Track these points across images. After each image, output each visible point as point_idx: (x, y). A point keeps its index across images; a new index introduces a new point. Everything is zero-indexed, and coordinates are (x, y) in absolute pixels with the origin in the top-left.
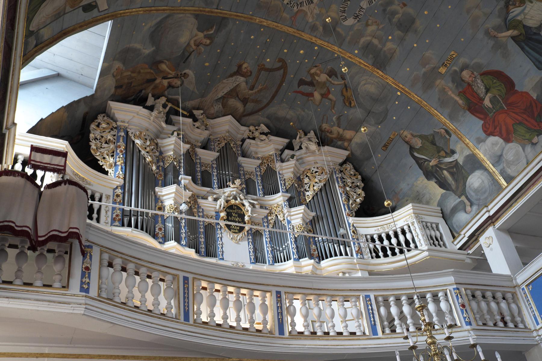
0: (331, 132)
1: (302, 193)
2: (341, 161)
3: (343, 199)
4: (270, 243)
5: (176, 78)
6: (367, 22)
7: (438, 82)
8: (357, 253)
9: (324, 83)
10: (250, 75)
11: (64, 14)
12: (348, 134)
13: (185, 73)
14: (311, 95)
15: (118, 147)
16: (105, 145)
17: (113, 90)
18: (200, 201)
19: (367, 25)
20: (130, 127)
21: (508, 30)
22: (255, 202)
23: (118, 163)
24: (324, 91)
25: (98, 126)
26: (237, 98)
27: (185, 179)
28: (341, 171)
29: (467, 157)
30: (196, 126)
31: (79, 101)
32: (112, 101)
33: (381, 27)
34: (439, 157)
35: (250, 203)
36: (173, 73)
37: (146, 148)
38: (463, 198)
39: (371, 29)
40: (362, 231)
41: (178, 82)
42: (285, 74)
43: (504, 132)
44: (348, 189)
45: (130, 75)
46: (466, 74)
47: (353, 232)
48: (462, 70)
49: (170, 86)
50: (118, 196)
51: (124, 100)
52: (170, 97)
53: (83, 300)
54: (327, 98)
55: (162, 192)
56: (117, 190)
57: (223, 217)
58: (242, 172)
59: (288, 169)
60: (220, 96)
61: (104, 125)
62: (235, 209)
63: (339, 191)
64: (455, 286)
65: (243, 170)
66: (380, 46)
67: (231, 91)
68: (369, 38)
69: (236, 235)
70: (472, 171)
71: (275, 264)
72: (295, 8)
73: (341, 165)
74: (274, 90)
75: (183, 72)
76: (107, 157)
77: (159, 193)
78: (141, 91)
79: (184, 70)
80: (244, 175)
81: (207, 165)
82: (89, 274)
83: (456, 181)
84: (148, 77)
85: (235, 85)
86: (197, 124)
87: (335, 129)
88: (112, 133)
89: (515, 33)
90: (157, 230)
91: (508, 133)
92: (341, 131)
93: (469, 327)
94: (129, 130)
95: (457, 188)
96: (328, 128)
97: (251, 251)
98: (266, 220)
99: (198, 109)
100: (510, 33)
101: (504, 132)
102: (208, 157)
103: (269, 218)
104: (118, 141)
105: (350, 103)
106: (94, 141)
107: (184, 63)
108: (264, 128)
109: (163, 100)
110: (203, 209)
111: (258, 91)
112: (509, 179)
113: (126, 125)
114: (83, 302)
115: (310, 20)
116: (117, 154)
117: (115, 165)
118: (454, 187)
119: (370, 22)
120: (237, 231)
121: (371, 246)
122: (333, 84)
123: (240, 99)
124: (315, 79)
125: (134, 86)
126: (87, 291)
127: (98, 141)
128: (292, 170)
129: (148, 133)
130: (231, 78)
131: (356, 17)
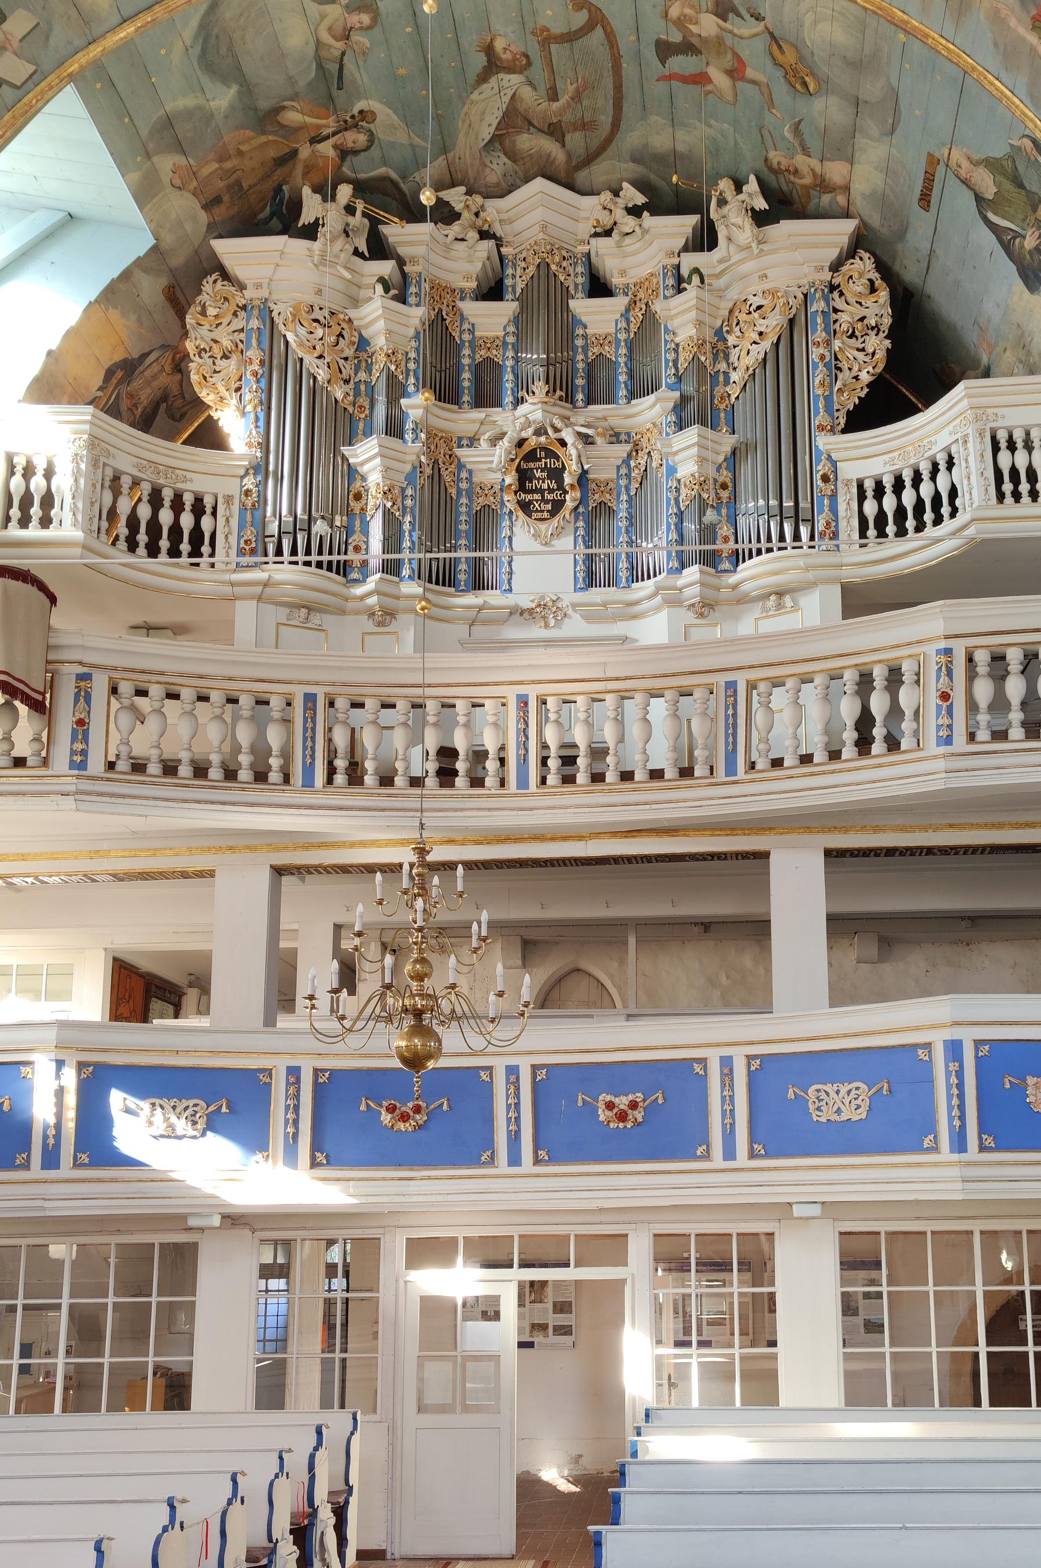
3: (817, 381)
4: (627, 532)
5: (346, 129)
9: (719, 41)
10: (529, 64)
13: (361, 112)
14: (701, 79)
16: (221, 364)
17: (203, 217)
20: (274, 297)
22: (590, 432)
24: (728, 61)
25: (203, 313)
26: (532, 129)
30: (451, 237)
31: (126, 275)
32: (220, 236)
35: (579, 434)
36: (330, 124)
37: (314, 348)
41: (355, 138)
42: (611, 38)
45: (221, 168)
47: (825, 479)
49: (344, 153)
51: (249, 226)
52: (362, 176)
54: (743, 79)
55: (356, 456)
57: (511, 485)
59: (682, 312)
61: (211, 311)
62: (540, 460)
67: (506, 115)
69: (543, 526)
71: (635, 585)
74: (608, 82)
75: (355, 111)
76: (227, 395)
77: (351, 461)
78: (278, 190)
79: (353, 105)
81: (490, 343)
84: (273, 153)
85: (506, 99)
92: (815, 163)
94: (272, 306)
98: (624, 471)
103: (632, 464)
105: (805, 84)
106: (197, 359)
107: (340, 88)
109: (345, 192)
110: (470, 472)
111: (572, 99)
113: (264, 293)
120: (546, 515)
122: (741, 38)
123: (540, 130)
124: (692, 34)
125: (250, 187)
127: (205, 356)
128: (693, 314)
129: (316, 301)
130: (485, 86)
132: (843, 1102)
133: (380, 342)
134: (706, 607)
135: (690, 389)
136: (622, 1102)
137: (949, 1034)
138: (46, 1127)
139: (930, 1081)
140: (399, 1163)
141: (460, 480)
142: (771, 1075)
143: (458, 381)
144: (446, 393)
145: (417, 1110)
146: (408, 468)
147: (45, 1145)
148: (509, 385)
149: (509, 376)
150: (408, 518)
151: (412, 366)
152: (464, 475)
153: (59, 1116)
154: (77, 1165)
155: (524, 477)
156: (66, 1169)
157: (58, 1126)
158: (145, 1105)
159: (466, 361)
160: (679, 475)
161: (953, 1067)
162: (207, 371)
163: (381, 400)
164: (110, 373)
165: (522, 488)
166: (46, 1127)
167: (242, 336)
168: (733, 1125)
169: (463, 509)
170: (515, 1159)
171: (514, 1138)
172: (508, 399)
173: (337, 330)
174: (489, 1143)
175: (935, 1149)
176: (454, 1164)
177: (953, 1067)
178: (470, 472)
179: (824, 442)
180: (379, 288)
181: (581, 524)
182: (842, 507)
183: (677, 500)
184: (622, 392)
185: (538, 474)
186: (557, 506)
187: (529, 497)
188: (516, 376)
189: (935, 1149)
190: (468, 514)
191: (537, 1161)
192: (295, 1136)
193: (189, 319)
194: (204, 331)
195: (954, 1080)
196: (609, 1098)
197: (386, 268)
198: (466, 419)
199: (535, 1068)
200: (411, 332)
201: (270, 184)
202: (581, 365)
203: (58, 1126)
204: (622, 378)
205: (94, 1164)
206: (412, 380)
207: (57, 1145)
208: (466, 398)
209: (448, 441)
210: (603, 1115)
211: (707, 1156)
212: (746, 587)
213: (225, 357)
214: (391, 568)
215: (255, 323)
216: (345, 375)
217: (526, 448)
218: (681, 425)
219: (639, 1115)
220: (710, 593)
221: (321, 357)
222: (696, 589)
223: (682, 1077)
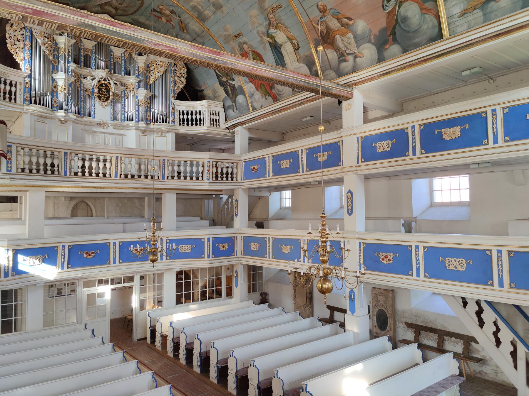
7: (232, 42)
8: (172, 121)
15: (25, 45)
16: (17, 43)
18: (83, 80)
21: (268, 37)
23: (26, 58)
25: (11, 26)
27: (72, 66)
28: (175, 64)
29: (239, 86)
34: (227, 78)
38: (234, 104)
40: (178, 108)
43: (256, 84)
44: (176, 78)
46: (245, 46)
47: (173, 108)
48: (244, 43)
50: (27, 83)
56: (26, 79)
58: (112, 57)
60: (98, 4)
63: (171, 79)
64: (208, 160)
66: (202, 10)
68: (196, 4)
69: (104, 103)
70: (240, 94)
82: (11, 162)
83: (233, 94)
88: (22, 32)
89: (271, 41)
91: (258, 86)
93: (208, 181)
95: (232, 97)
100: (268, 39)
101: (256, 84)
104: (26, 40)
106: (9, 39)
112: (254, 109)
114: (9, 177)
116: (26, 51)
117: (24, 59)
118: (231, 96)
121: (181, 117)
126: (10, 171)
127: (12, 39)
132: (187, 249)
134: (144, 132)
137: (208, 237)
138: (5, 267)
139: (204, 245)
140: (88, 266)
141: (81, 86)
144: (77, 62)
146: (70, 82)
153: (8, 263)
154: (12, 275)
157: (8, 266)
158: (28, 258)
163: (62, 61)
166: (5, 267)
170: (114, 262)
171: (115, 258)
174: (109, 259)
175: (204, 258)
176: (100, 265)
182: (176, 116)
186: (107, 99)
189: (204, 258)
191: (119, 263)
198: (85, 71)
199: (119, 242)
205: (16, 274)
207: (8, 271)
219: (142, 252)
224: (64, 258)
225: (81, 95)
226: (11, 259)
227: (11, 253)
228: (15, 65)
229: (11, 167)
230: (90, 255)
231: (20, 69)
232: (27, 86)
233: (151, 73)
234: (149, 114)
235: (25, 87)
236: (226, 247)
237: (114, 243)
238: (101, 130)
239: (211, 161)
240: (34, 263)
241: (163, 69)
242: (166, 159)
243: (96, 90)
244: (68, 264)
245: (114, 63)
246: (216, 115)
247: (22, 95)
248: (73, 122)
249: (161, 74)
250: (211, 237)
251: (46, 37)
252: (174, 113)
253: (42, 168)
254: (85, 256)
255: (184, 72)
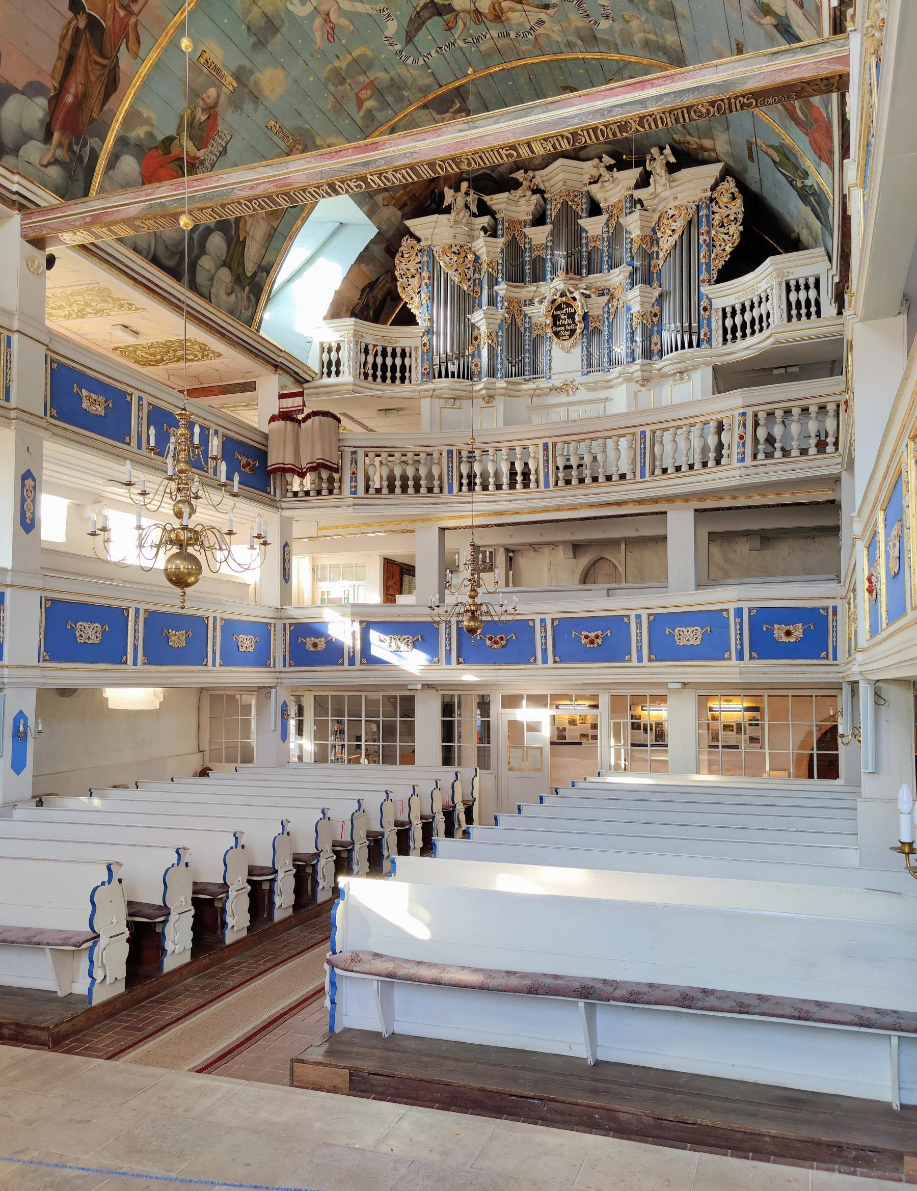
0: (688, 143)
1: (655, 255)
2: (712, 181)
6: (624, 19)
11: (275, 229)
12: (707, 143)
17: (399, 213)
19: (628, 22)
20: (434, 243)
22: (587, 292)
23: (424, 302)
25: (402, 256)
27: (502, 289)
33: (643, 19)
39: (635, 24)
40: (718, 304)
50: (425, 345)
53: (351, 501)
61: (406, 256)
64: (741, 411)
65: (587, 238)
68: (641, 35)
69: (566, 343)
72: (529, 36)
73: (713, 189)
78: (433, 192)
80: (587, 244)
82: (356, 478)
86: (520, 192)
87: (689, 138)
90: (474, 368)
93: (739, 464)
96: (682, 140)
97: (585, 358)
99: (518, 169)
102: (539, 235)
108: (608, 160)
109: (464, 186)
110: (530, 318)
113: (429, 243)
114: (351, 503)
115: (559, 39)
119: (627, 18)
121: (729, 323)
126: (355, 493)
131: (607, 17)
132: (690, 636)
133: (484, 258)
134: (645, 381)
135: (637, 263)
136: (592, 635)
137: (736, 605)
138: (349, 648)
139: (729, 626)
140: (495, 663)
142: (662, 624)
143: (524, 270)
145: (502, 639)
146: (499, 321)
147: (349, 656)
148: (549, 269)
149: (549, 264)
150: (500, 348)
151: (500, 267)
152: (527, 320)
153: (354, 644)
154: (362, 663)
155: (556, 318)
156: (358, 665)
158: (388, 638)
159: (527, 259)
160: (632, 312)
161: (738, 620)
162: (405, 285)
163: (485, 287)
164: (363, 290)
165: (555, 325)
166: (349, 648)
167: (420, 265)
168: (641, 646)
169: (527, 338)
170: (545, 661)
171: (545, 651)
172: (548, 277)
173: (463, 254)
174: (534, 654)
177: (738, 620)
178: (530, 318)
179: (705, 289)
180: (482, 233)
181: (585, 340)
182: (713, 324)
183: (631, 325)
184: (606, 267)
185: (563, 317)
186: (573, 332)
187: (558, 329)
188: (552, 264)
190: (530, 340)
191: (555, 662)
192: (450, 650)
193: (396, 261)
194: (403, 265)
195: (738, 627)
196: (586, 633)
197: (485, 220)
198: (526, 291)
199: (553, 619)
200: (499, 250)
201: (429, 191)
202: (584, 254)
203: (354, 648)
204: (606, 259)
206: (500, 275)
207: (354, 655)
208: (527, 279)
209: (519, 303)
210: (584, 641)
211: (630, 660)
212: (664, 370)
213: (413, 277)
214: (492, 373)
215: (425, 259)
216: (468, 277)
217: (557, 304)
218: (632, 285)
220: (646, 374)
221: (456, 270)
222: (639, 373)
223: (618, 624)
224: (450, 644)
225: (525, 340)
226: (358, 636)
227: (357, 627)
228: (407, 319)
229: (356, 487)
230: (496, 642)
231: (417, 324)
232: (425, 349)
233: (661, 244)
234: (655, 339)
235: (423, 353)
236: (798, 632)
237: (543, 621)
238: (564, 399)
239: (750, 412)
240: (399, 647)
241: (679, 225)
242: (648, 430)
243: (549, 321)
244: (459, 655)
245: (589, 254)
246: (807, 287)
247: (419, 368)
248: (505, 395)
249: (676, 236)
250: (745, 606)
251: (454, 253)
252: (709, 318)
253: (411, 483)
254: (488, 642)
255: (737, 208)
